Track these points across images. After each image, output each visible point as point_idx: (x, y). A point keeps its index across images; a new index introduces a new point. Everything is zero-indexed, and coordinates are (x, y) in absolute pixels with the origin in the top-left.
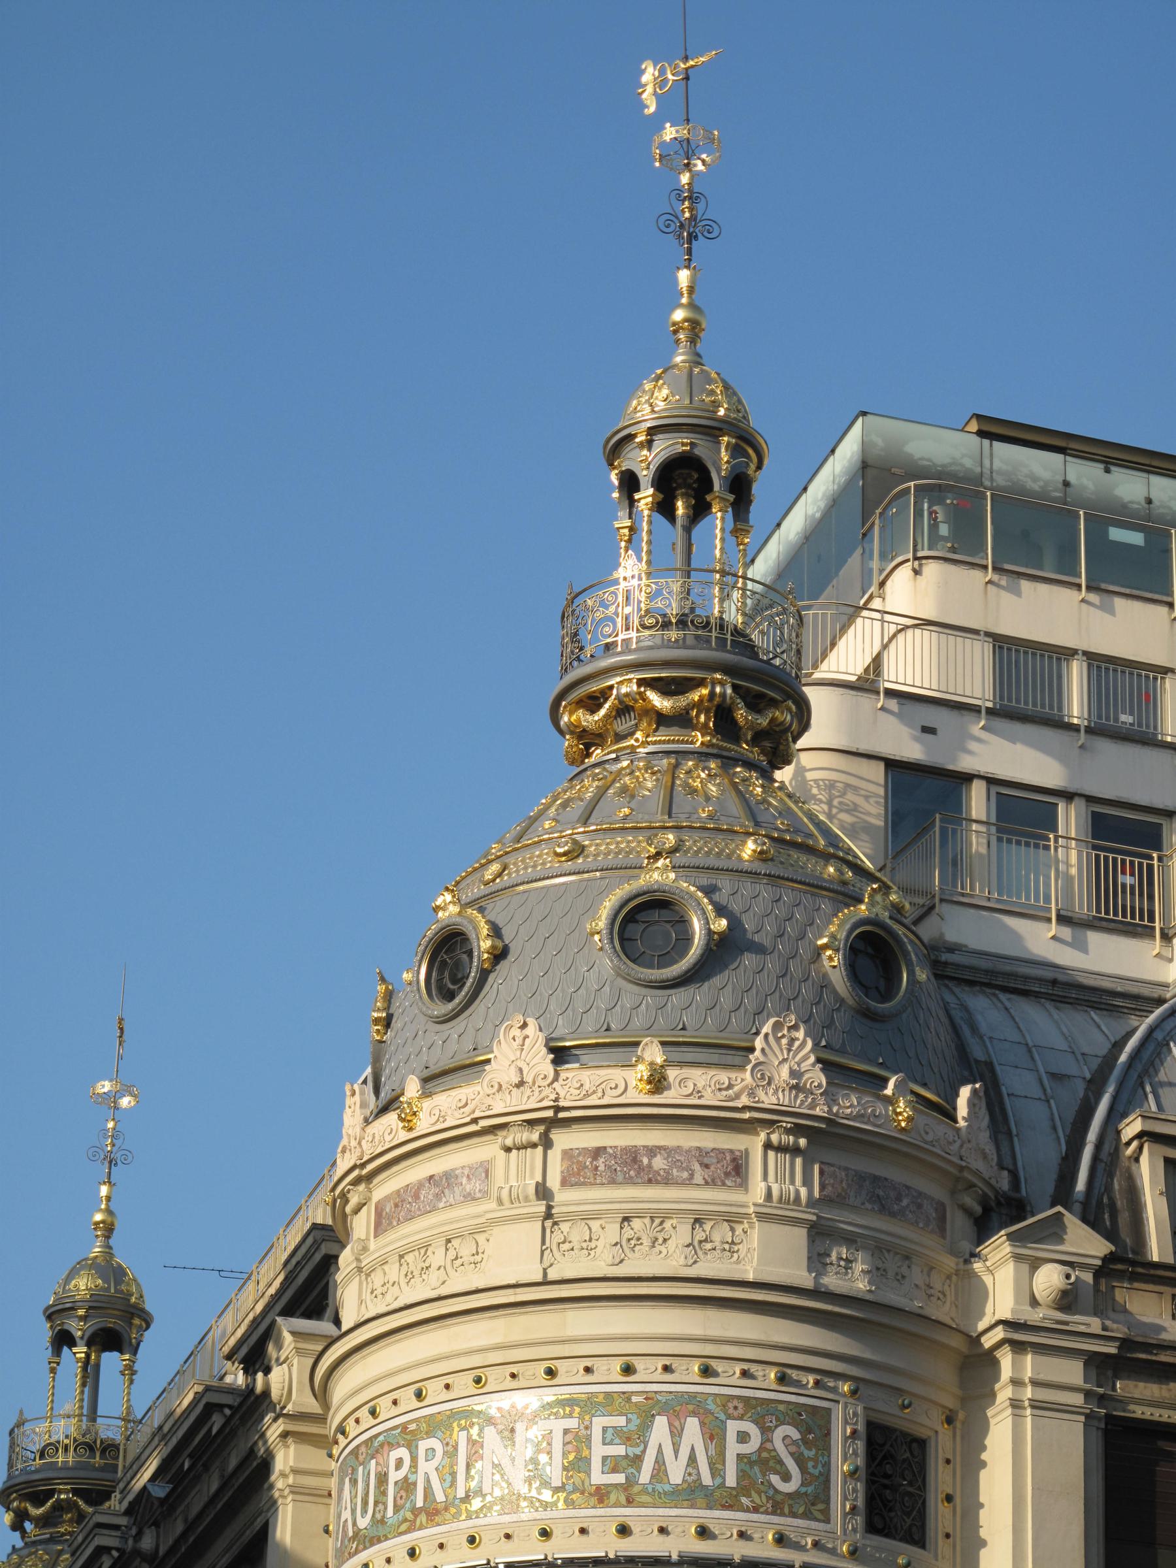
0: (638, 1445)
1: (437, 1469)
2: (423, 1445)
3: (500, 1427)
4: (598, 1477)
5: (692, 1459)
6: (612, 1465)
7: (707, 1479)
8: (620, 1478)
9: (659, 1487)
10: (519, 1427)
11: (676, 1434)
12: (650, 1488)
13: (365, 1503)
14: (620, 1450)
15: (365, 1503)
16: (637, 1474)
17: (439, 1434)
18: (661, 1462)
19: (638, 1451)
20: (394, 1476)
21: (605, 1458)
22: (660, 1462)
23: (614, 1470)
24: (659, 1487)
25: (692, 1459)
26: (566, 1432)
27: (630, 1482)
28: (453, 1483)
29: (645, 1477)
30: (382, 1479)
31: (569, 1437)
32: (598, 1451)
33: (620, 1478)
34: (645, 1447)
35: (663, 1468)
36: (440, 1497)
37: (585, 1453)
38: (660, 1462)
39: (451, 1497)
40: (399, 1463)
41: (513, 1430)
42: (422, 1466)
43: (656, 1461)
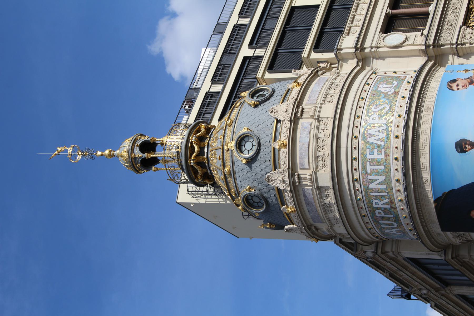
0: (375, 146)
1: (380, 202)
2: (375, 206)
3: (369, 183)
4: (382, 156)
5: (379, 131)
6: (379, 152)
7: (384, 128)
8: (383, 150)
10: (370, 177)
12: (386, 142)
13: (389, 224)
14: (376, 150)
15: (389, 224)
17: (372, 201)
19: (376, 146)
20: (383, 215)
21: (378, 154)
22: (379, 140)
23: (381, 152)
24: (386, 140)
25: (379, 131)
26: (370, 165)
28: (383, 196)
29: (383, 143)
30: (383, 218)
31: (372, 164)
32: (375, 156)
33: (383, 150)
34: (375, 143)
36: (387, 200)
38: (379, 140)
39: (388, 197)
40: (379, 213)
41: (370, 179)
42: (380, 206)
43: (379, 141)
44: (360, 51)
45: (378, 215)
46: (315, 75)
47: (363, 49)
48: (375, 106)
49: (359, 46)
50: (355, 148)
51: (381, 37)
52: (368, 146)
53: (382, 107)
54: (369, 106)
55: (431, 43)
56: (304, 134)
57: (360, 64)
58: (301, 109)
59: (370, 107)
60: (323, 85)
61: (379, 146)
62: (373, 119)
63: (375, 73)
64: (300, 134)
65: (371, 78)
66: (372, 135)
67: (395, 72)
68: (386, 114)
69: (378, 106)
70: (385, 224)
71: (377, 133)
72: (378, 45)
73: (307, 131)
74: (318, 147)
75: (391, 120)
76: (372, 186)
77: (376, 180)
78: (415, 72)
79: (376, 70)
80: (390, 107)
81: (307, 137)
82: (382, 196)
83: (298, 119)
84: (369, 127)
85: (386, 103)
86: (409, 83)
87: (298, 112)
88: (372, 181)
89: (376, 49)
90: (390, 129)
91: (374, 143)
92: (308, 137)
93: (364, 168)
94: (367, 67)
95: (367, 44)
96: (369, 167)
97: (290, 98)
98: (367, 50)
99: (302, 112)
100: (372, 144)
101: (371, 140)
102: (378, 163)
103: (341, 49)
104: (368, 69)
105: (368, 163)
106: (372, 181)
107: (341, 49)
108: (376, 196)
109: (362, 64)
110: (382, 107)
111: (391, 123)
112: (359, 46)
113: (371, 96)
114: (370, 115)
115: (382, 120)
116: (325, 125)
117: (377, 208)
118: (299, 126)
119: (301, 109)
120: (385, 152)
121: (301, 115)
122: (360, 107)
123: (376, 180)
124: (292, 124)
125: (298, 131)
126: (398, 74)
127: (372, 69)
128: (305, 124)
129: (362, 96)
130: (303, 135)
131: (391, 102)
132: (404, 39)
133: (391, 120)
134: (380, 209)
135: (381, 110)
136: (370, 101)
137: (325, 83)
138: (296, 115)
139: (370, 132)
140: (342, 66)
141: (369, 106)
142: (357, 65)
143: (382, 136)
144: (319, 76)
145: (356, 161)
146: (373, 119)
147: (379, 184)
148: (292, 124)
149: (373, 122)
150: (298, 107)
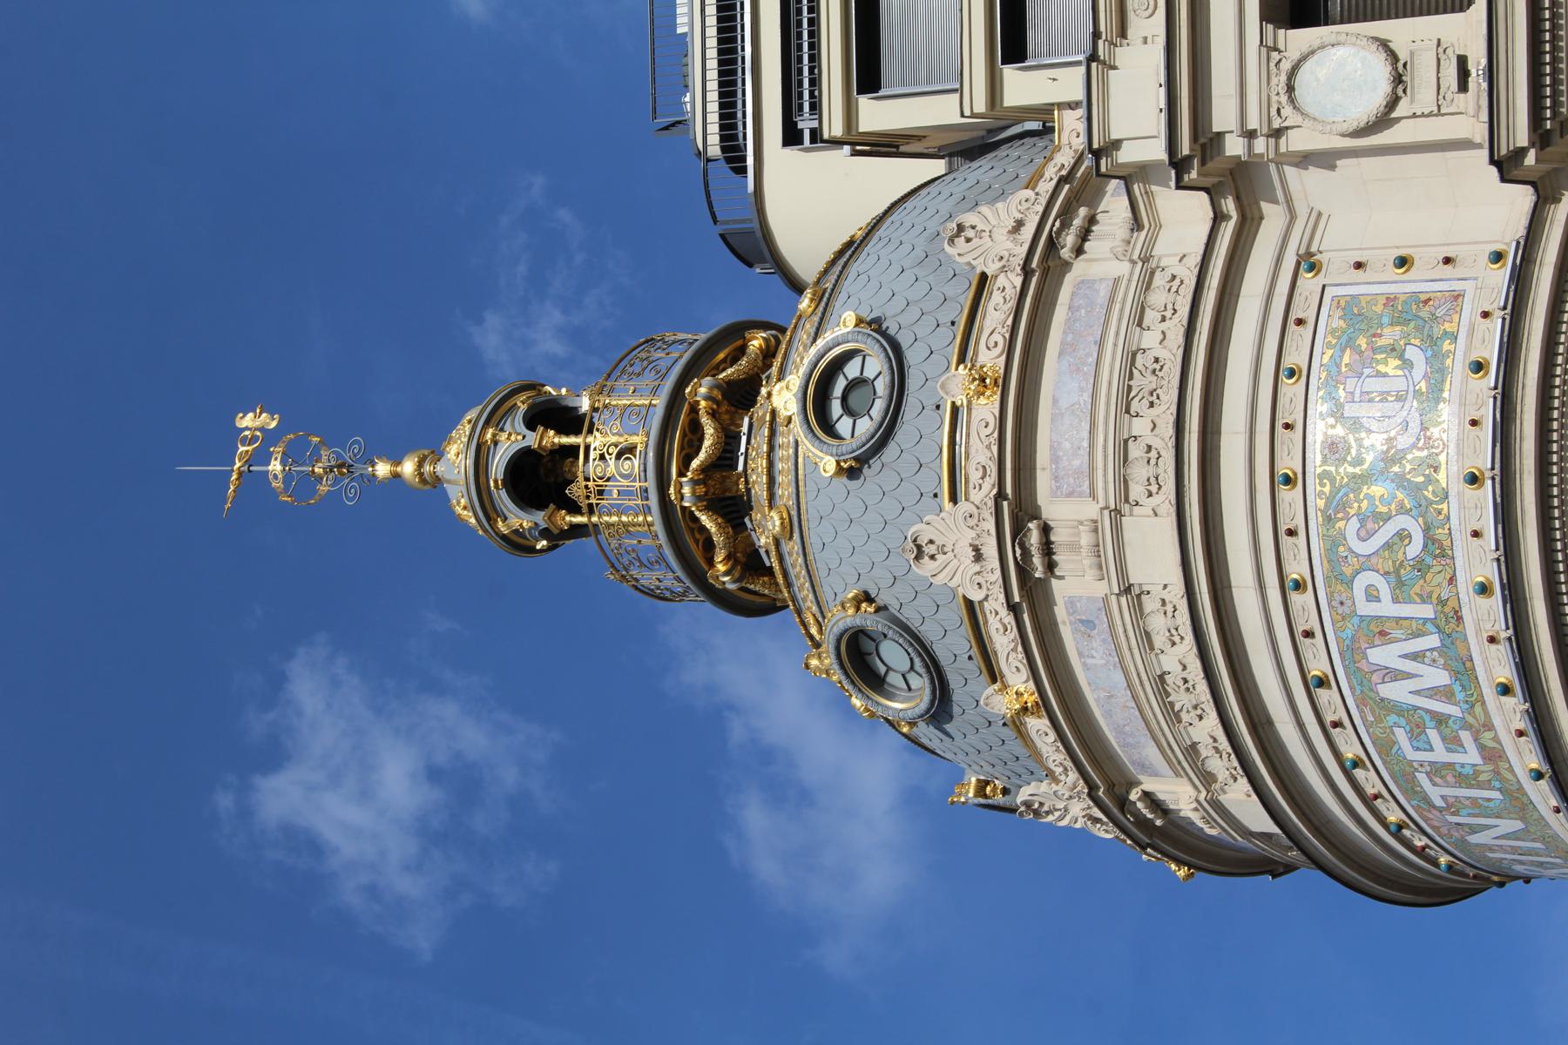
4: (1472, 756)
5: (1415, 657)
6: (1453, 743)
8: (1465, 736)
9: (1460, 696)
14: (1433, 734)
16: (1453, 719)
18: (1430, 692)
25: (1415, 657)
27: (1467, 726)
32: (1440, 754)
33: (1465, 736)
35: (1442, 689)
43: (1430, 697)
44: (1203, 163)
46: (1045, 272)
47: (1208, 143)
48: (1354, 524)
49: (1185, 148)
50: (1336, 725)
51: (1272, 65)
52: (1393, 718)
54: (1329, 520)
55: (1522, 138)
56: (1093, 652)
57: (1229, 205)
58: (1034, 538)
59: (1337, 526)
60: (1092, 360)
61: (1440, 720)
63: (1312, 267)
64: (1080, 654)
65: (1300, 322)
67: (1402, 262)
69: (1370, 525)
71: (1409, 666)
72: (1276, 125)
73: (1104, 641)
74: (1176, 710)
78: (1498, 257)
79: (1309, 246)
81: (1112, 668)
83: (1044, 585)
85: (1402, 511)
86: (1478, 367)
87: (1026, 553)
89: (1271, 141)
91: (1416, 708)
92: (1115, 665)
93: (1412, 789)
94: (1265, 207)
95: (1223, 116)
96: (1435, 794)
97: (975, 476)
98: (1234, 147)
99: (1048, 549)
102: (1463, 780)
103: (1117, 144)
104: (1273, 218)
105: (1422, 778)
107: (1117, 144)
109: (1238, 199)
112: (1185, 148)
113: (1325, 461)
114: (1348, 571)
116: (1165, 613)
118: (1060, 612)
119: (1034, 538)
120: (1482, 748)
121: (1050, 566)
122: (1291, 533)
124: (1026, 617)
125: (1063, 635)
126: (1422, 280)
127: (1293, 217)
128: (1078, 605)
129: (1281, 470)
130: (1093, 657)
131: (1424, 503)
132: (1389, 89)
136: (1327, 489)
137: (1101, 344)
138: (1024, 572)
140: (1151, 204)
142: (1218, 218)
143: (1439, 677)
144: (1066, 266)
145: (1364, 767)
148: (1026, 617)
150: (1019, 530)
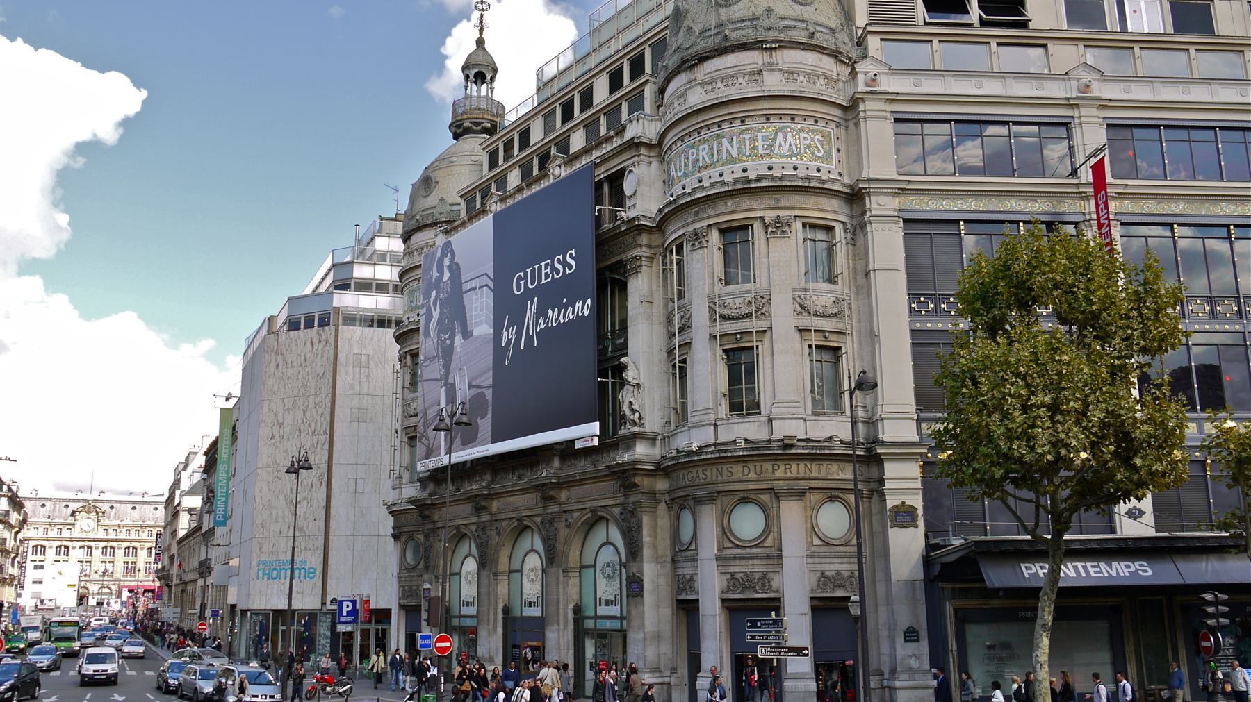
2: (701, 147)
4: (761, 151)
5: (790, 145)
7: (795, 152)
8: (768, 152)
11: (785, 137)
14: (768, 143)
21: (763, 146)
22: (780, 146)
25: (790, 145)
32: (760, 144)
33: (768, 152)
37: (757, 144)
40: (693, 154)
42: (701, 153)
45: (690, 152)
53: (820, 147)
54: (821, 132)
62: (805, 138)
66: (785, 137)
68: (813, 153)
70: (680, 162)
71: (788, 144)
75: (805, 159)
76: (725, 142)
77: (732, 146)
80: (819, 157)
82: (713, 155)
84: (795, 133)
88: (731, 142)
90: (794, 158)
96: (747, 136)
100: (775, 139)
101: (780, 135)
106: (731, 142)
108: (712, 148)
110: (821, 149)
111: (802, 159)
115: (805, 149)
117: (698, 150)
123: (732, 146)
133: (805, 159)
134: (698, 155)
135: (817, 147)
139: (789, 134)
141: (821, 132)
146: (805, 138)
147: (727, 151)
149: (802, 139)
